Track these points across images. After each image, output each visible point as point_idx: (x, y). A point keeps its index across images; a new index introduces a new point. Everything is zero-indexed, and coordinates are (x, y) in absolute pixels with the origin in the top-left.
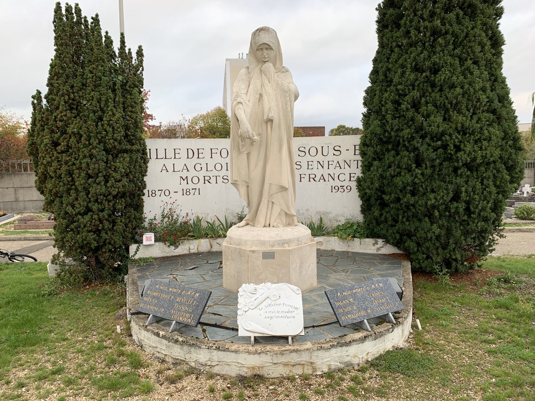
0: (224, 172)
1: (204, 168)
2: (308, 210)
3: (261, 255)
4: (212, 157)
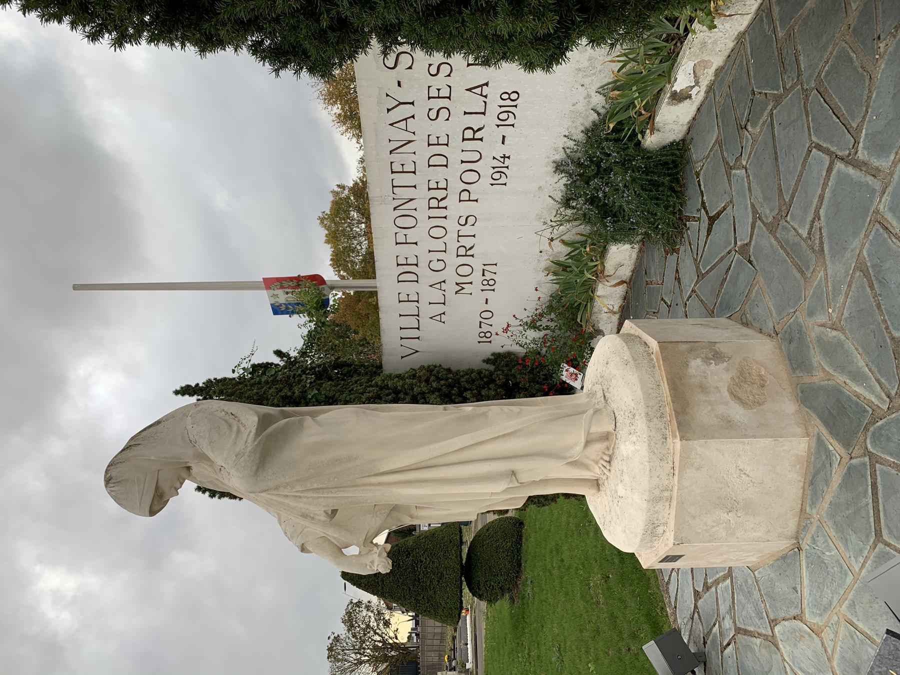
1: (441, 256)
4: (416, 243)
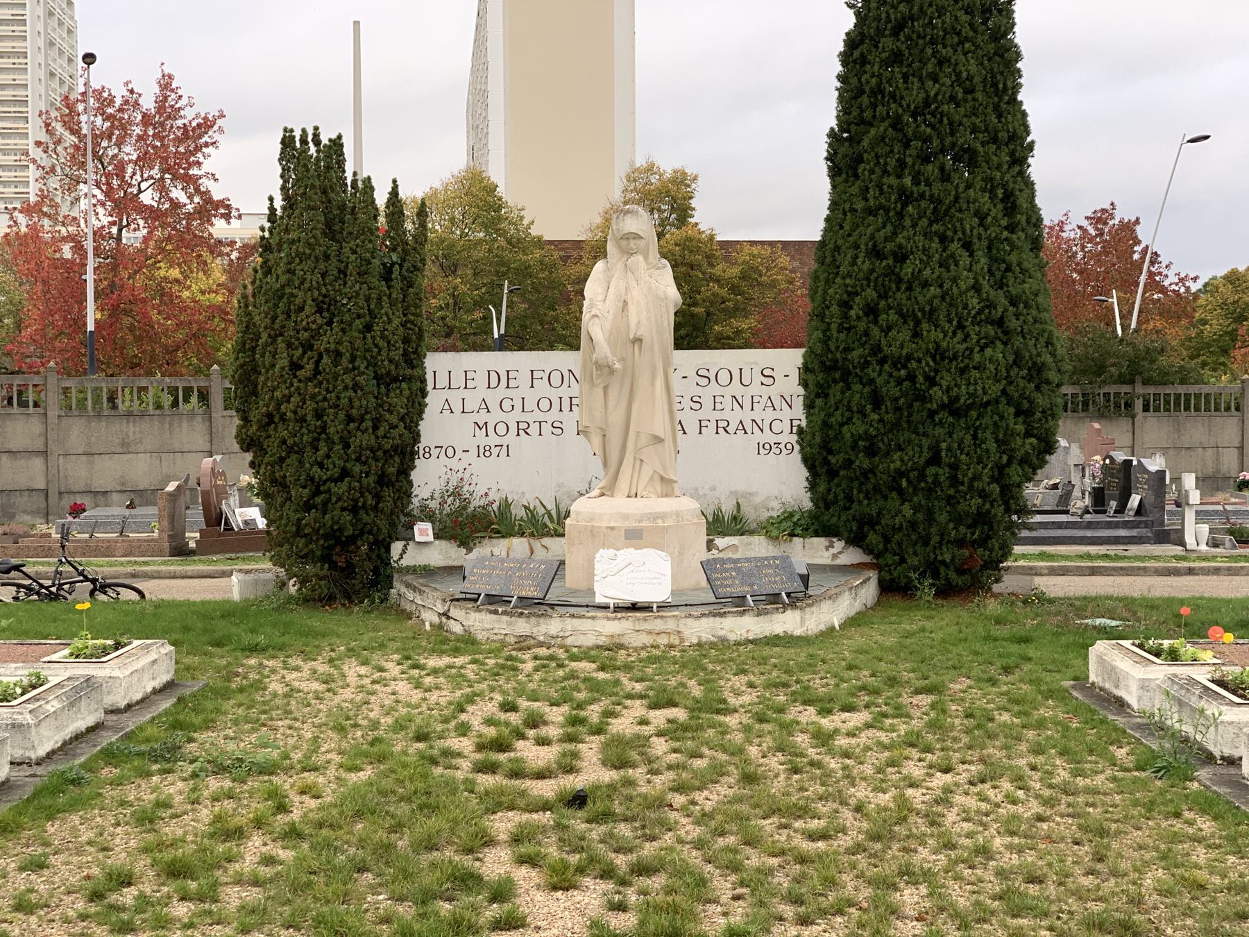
0: (554, 415)
1: (518, 407)
2: (713, 489)
3: (623, 532)
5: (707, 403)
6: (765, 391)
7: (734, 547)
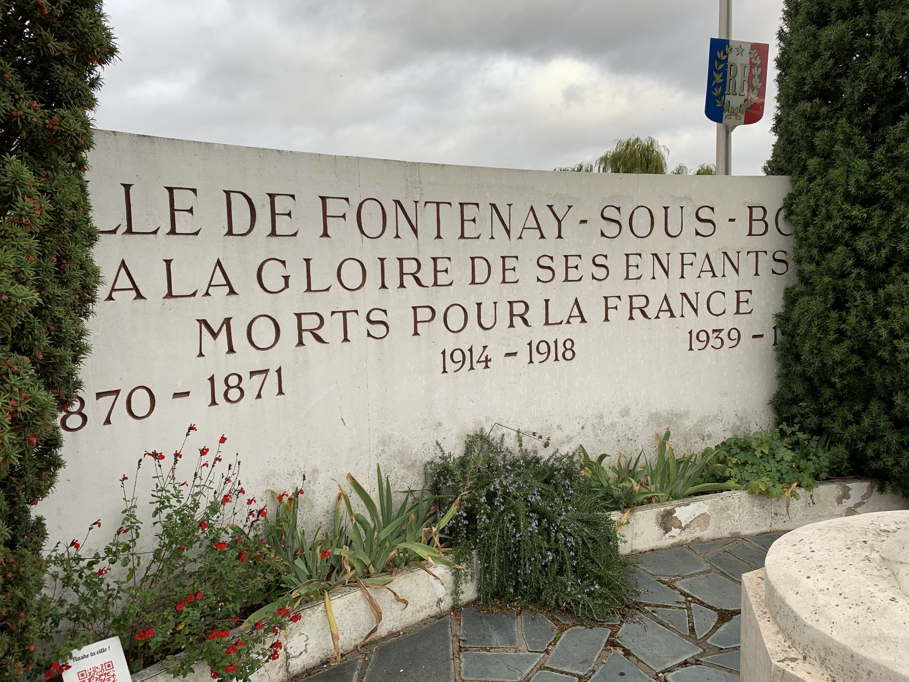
0: (370, 297)
2: (625, 413)
4: (325, 234)
5: (617, 266)
6: (702, 246)
7: (703, 519)
